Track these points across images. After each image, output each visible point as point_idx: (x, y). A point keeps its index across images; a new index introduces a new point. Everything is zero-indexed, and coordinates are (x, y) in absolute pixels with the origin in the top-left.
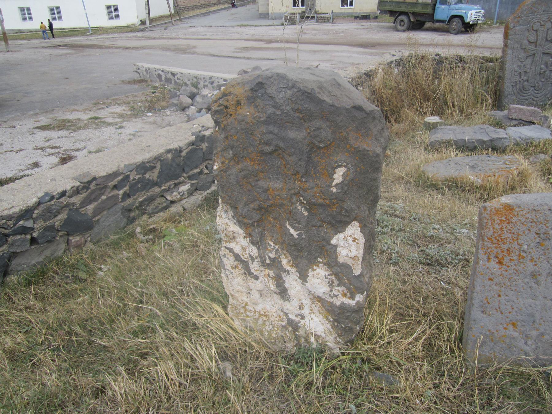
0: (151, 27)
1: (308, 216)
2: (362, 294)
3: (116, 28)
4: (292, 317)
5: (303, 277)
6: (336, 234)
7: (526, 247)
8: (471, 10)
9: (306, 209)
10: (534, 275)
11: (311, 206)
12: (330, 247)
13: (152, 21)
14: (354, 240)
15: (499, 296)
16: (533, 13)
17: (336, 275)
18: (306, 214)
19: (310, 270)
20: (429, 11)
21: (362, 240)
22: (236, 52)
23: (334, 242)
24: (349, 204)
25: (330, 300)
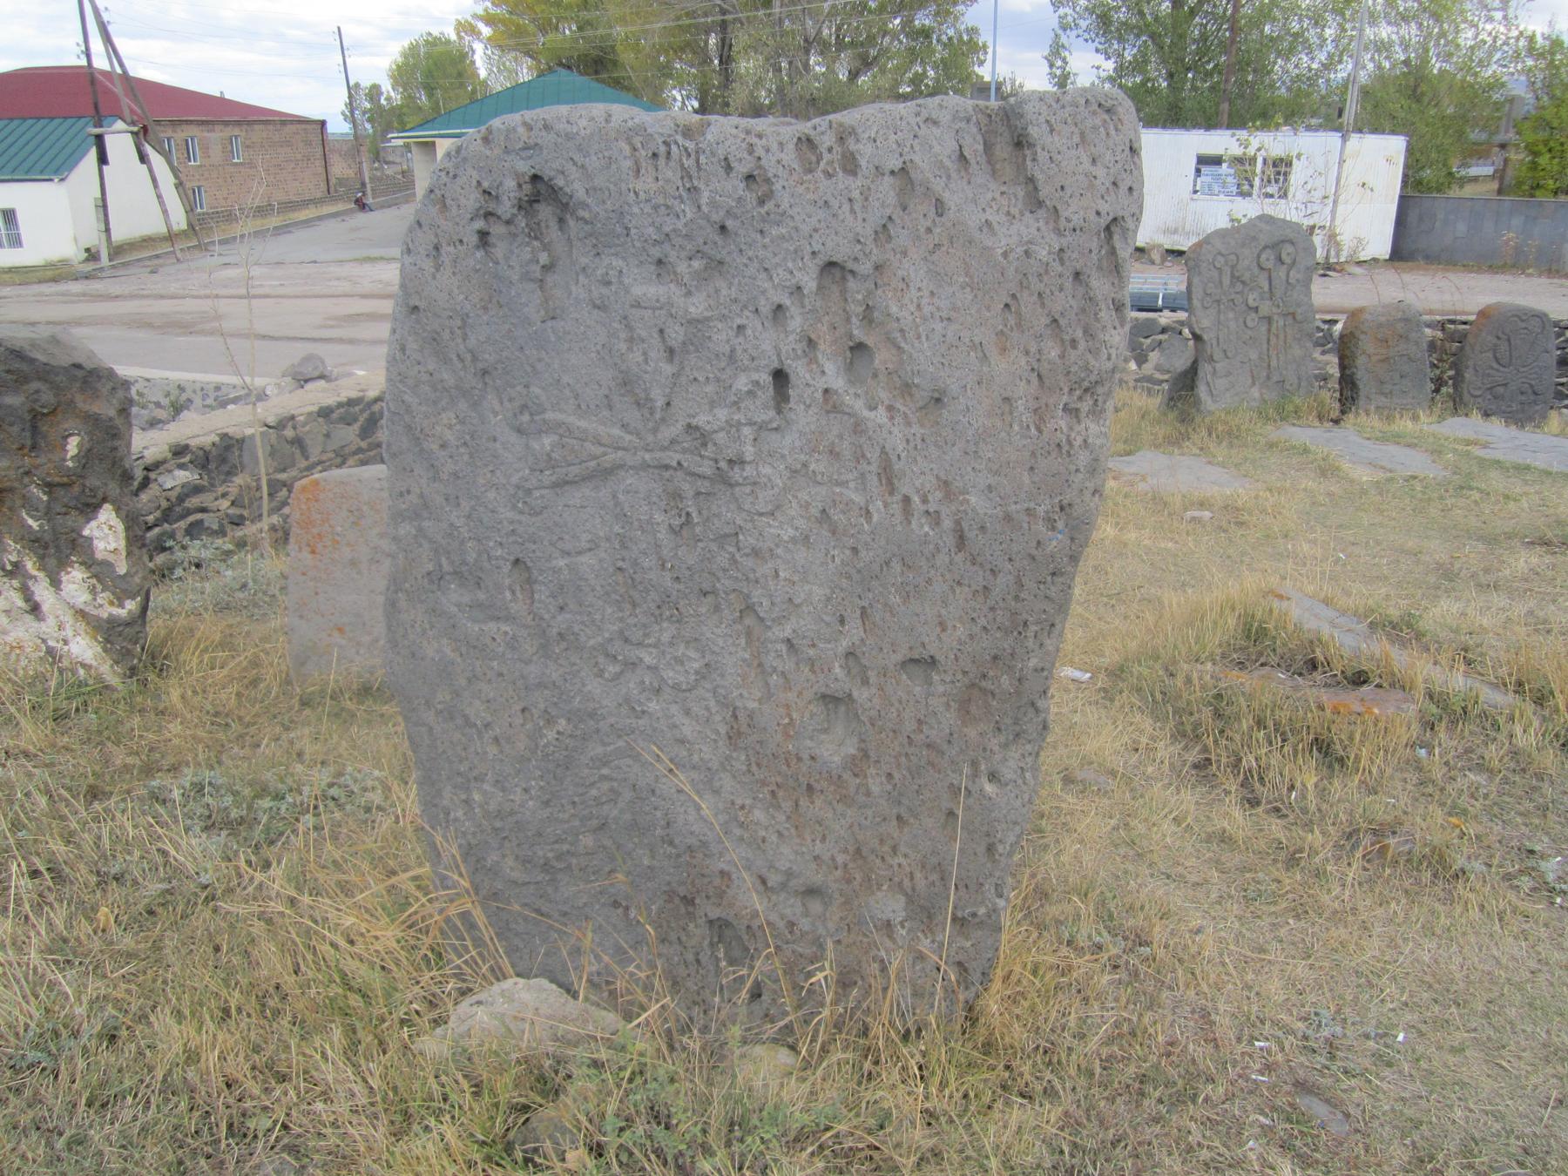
0: (113, 267)
1: (49, 502)
2: (133, 599)
3: (11, 270)
4: (52, 643)
5: (56, 583)
6: (88, 522)
7: (339, 529)
9: (45, 493)
10: (353, 563)
11: (49, 487)
12: (82, 540)
13: (117, 251)
14: (111, 527)
15: (317, 594)
17: (95, 576)
18: (45, 498)
19: (63, 573)
21: (120, 527)
22: (326, 327)
23: (86, 532)
24: (93, 481)
25: (95, 612)
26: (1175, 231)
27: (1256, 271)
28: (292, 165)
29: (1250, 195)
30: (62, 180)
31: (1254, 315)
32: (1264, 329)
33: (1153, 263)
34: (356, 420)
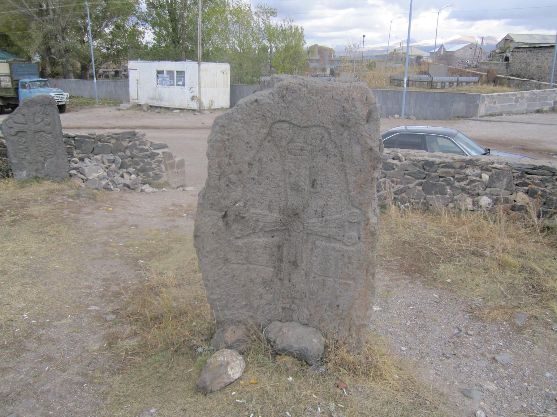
26: (153, 99)
29: (174, 85)
33: (144, 111)
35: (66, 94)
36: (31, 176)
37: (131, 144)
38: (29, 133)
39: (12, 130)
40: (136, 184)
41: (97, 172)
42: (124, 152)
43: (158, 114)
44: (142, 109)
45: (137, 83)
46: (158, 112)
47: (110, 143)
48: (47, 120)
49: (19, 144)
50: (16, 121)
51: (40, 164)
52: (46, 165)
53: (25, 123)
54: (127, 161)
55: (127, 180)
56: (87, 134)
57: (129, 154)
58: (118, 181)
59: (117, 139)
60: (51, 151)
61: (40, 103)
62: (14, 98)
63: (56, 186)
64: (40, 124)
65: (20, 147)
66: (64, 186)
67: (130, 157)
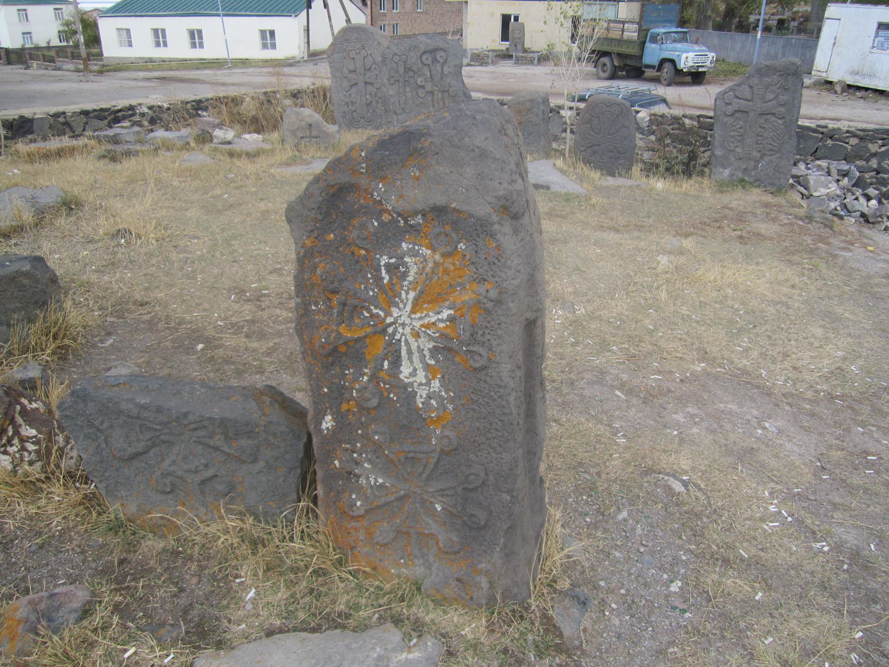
8: (688, 52)
16: (347, 40)
20: (633, 51)
26: (857, 73)
27: (420, 65)
28: (450, 14)
30: (296, 16)
31: (422, 90)
32: (429, 98)
33: (836, 93)
34: (106, 119)
35: (711, 55)
36: (734, 177)
37: (883, 149)
38: (752, 114)
39: (730, 107)
40: (881, 216)
41: (826, 187)
42: (867, 160)
43: (862, 101)
44: (833, 89)
45: (834, 44)
46: (861, 98)
47: (847, 143)
48: (783, 98)
49: (733, 128)
50: (738, 95)
51: (752, 163)
52: (760, 165)
53: (749, 99)
54: (867, 176)
55: (862, 205)
56: (813, 126)
57: (875, 166)
58: (853, 206)
59: (861, 139)
60: (775, 144)
61: (780, 71)
62: (635, 56)
63: (769, 199)
64: (771, 103)
65: (732, 134)
66: (780, 200)
67: (875, 170)
